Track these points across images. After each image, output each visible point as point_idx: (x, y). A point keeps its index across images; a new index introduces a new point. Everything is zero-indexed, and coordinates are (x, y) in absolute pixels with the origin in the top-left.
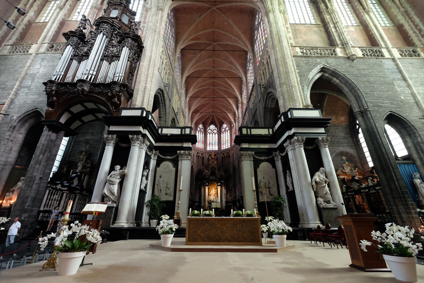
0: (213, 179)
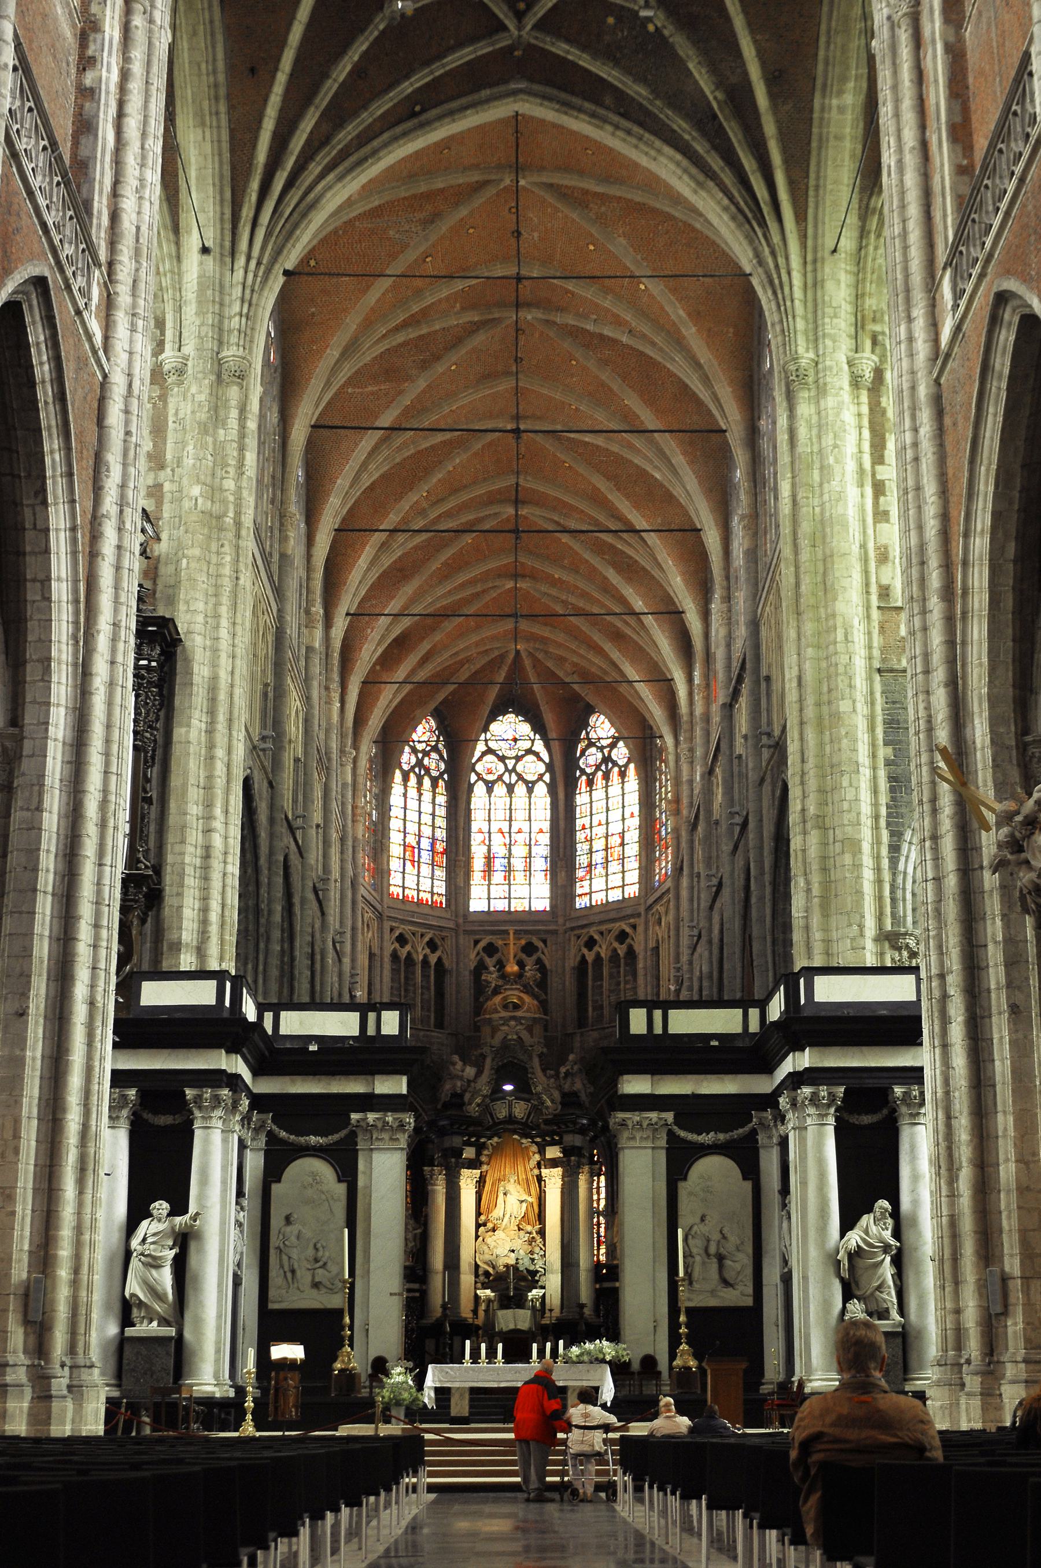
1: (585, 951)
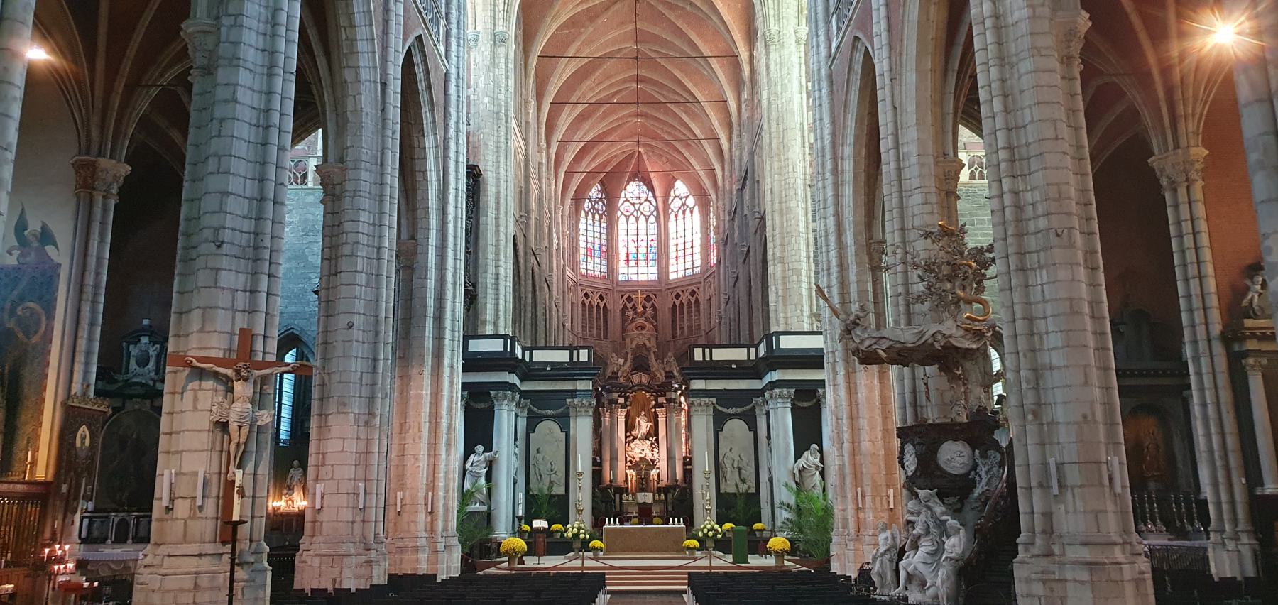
0: (640, 384)
1: (675, 300)
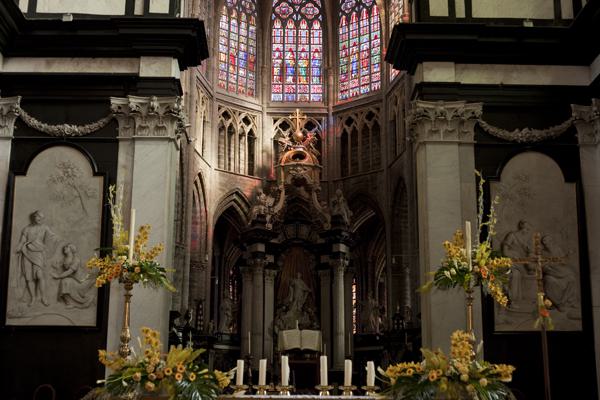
1: (346, 127)
